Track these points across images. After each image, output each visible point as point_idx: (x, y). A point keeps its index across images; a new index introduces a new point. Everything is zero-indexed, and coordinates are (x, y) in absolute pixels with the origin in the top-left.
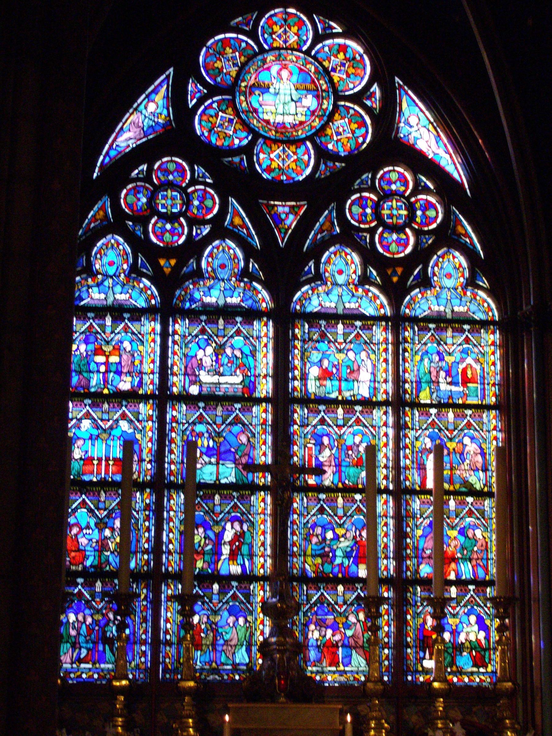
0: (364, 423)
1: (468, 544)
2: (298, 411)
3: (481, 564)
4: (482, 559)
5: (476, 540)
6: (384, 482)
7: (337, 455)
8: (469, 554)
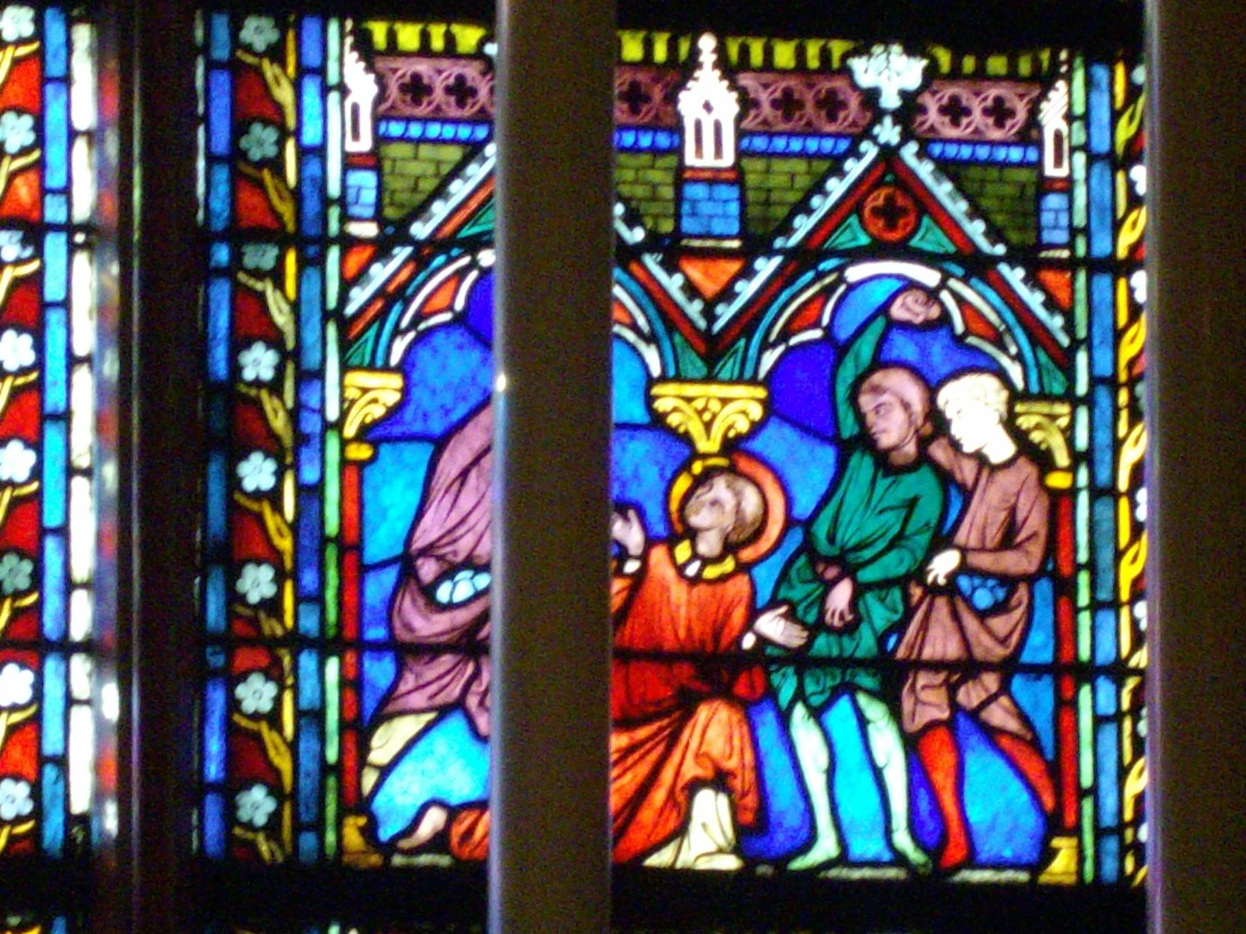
1: (863, 514)
3: (998, 715)
4: (1009, 668)
5: (946, 478)
8: (880, 614)
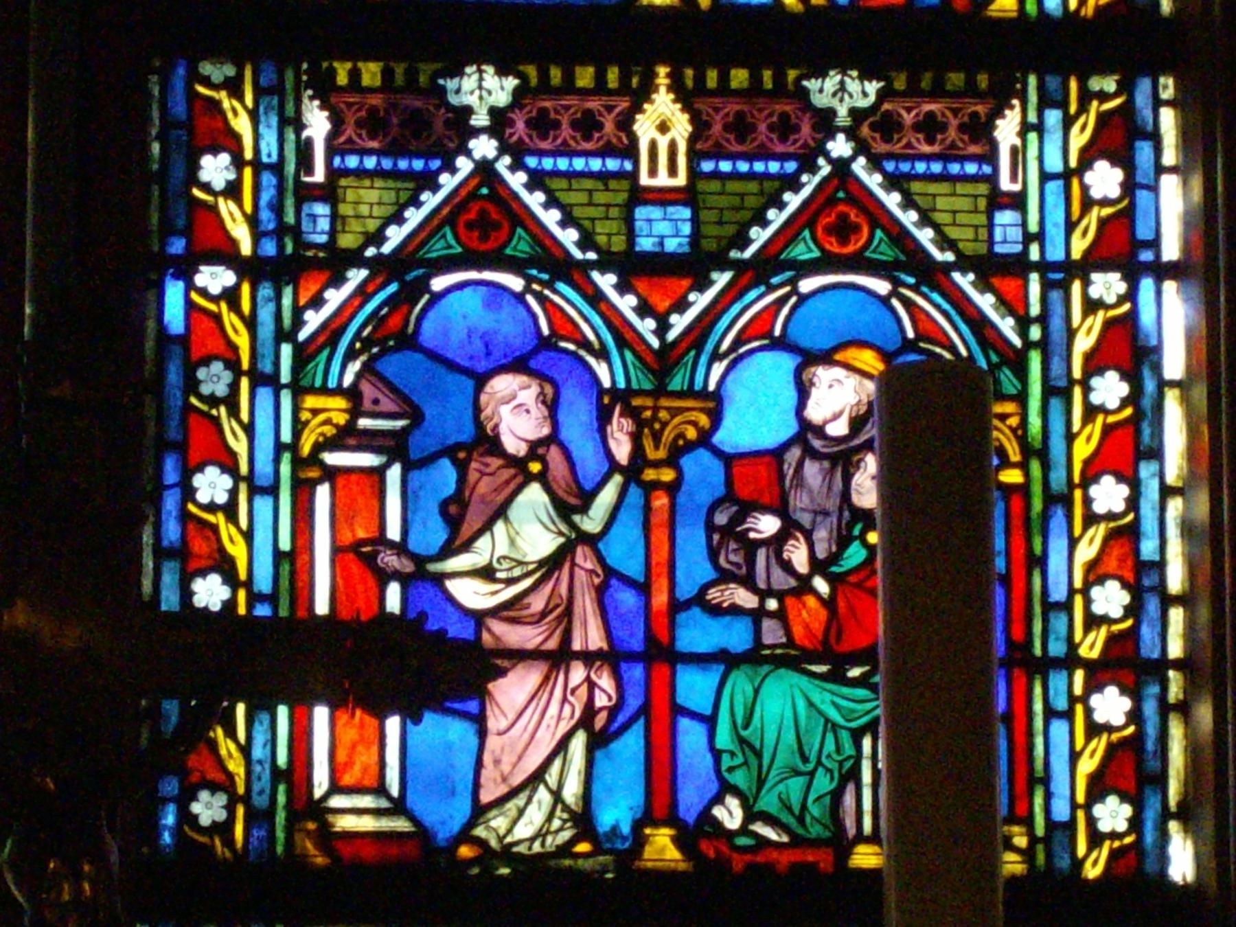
0: (900, 236)
2: (242, 124)
6: (1113, 814)
7: (625, 550)
